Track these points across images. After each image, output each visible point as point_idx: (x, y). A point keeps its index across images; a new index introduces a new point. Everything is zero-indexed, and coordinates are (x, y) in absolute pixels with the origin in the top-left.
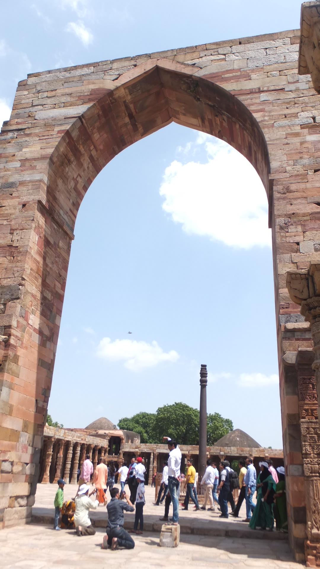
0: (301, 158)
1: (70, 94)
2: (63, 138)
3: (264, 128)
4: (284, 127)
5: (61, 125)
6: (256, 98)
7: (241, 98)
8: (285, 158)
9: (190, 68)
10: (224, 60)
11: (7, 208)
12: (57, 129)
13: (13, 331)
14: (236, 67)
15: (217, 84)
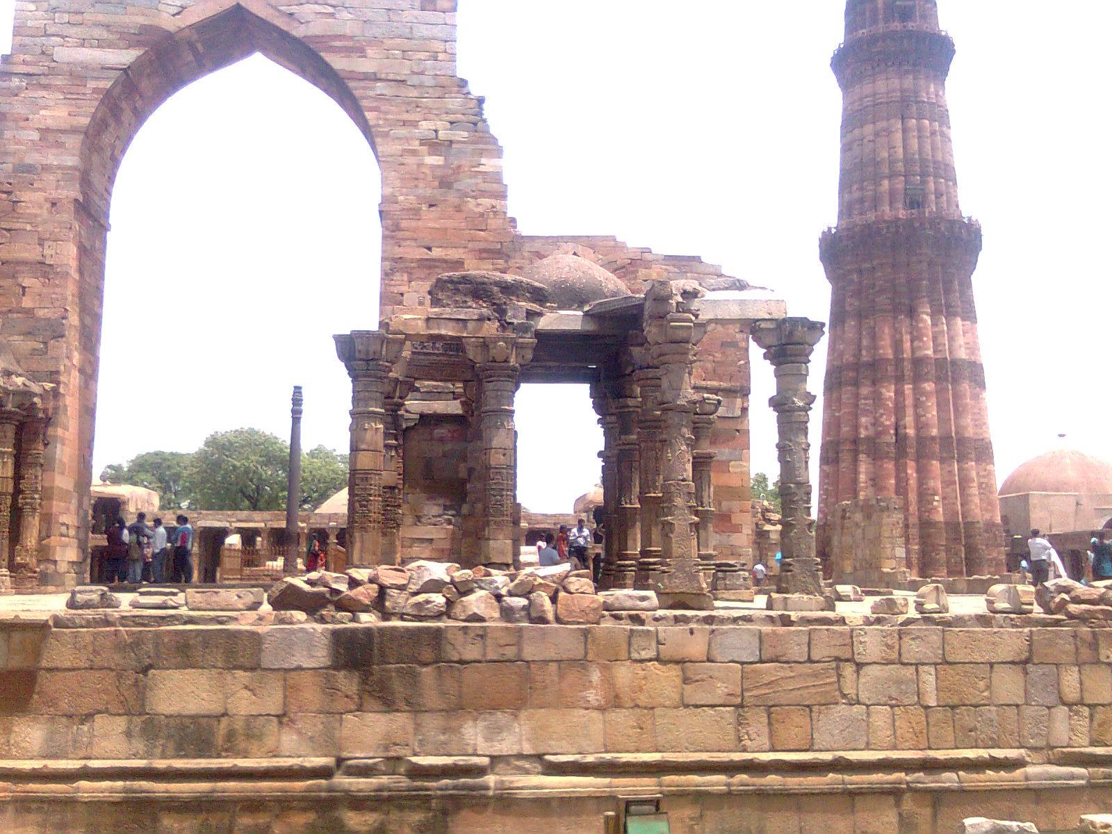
0: (416, 186)
1: (107, 26)
2: (102, 101)
3: (377, 136)
4: (401, 139)
5: (97, 78)
6: (373, 89)
7: (351, 84)
8: (398, 183)
9: (286, 19)
10: (332, 15)
11: (29, 205)
12: (92, 84)
13: (62, 378)
14: (348, 32)
15: (322, 54)
